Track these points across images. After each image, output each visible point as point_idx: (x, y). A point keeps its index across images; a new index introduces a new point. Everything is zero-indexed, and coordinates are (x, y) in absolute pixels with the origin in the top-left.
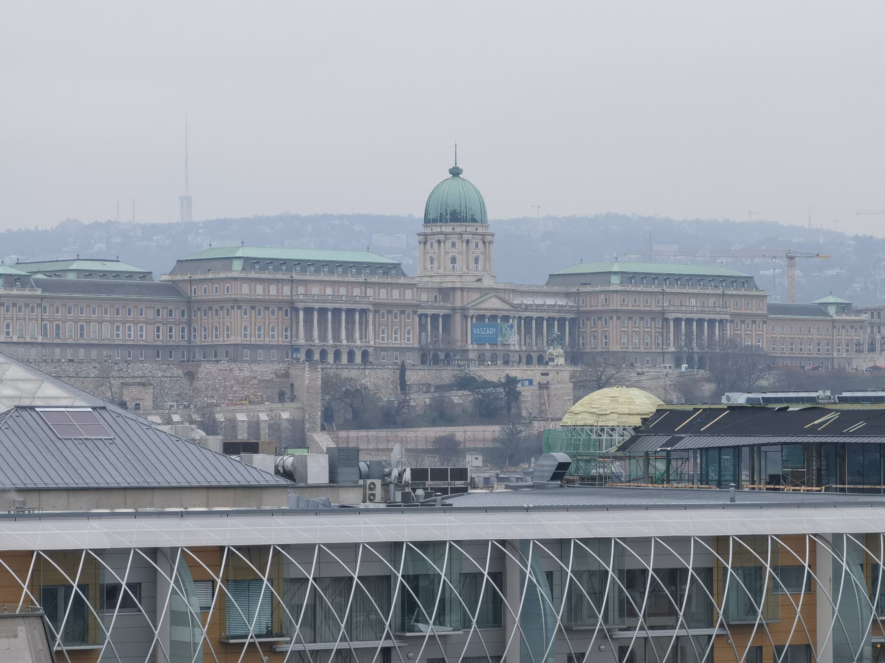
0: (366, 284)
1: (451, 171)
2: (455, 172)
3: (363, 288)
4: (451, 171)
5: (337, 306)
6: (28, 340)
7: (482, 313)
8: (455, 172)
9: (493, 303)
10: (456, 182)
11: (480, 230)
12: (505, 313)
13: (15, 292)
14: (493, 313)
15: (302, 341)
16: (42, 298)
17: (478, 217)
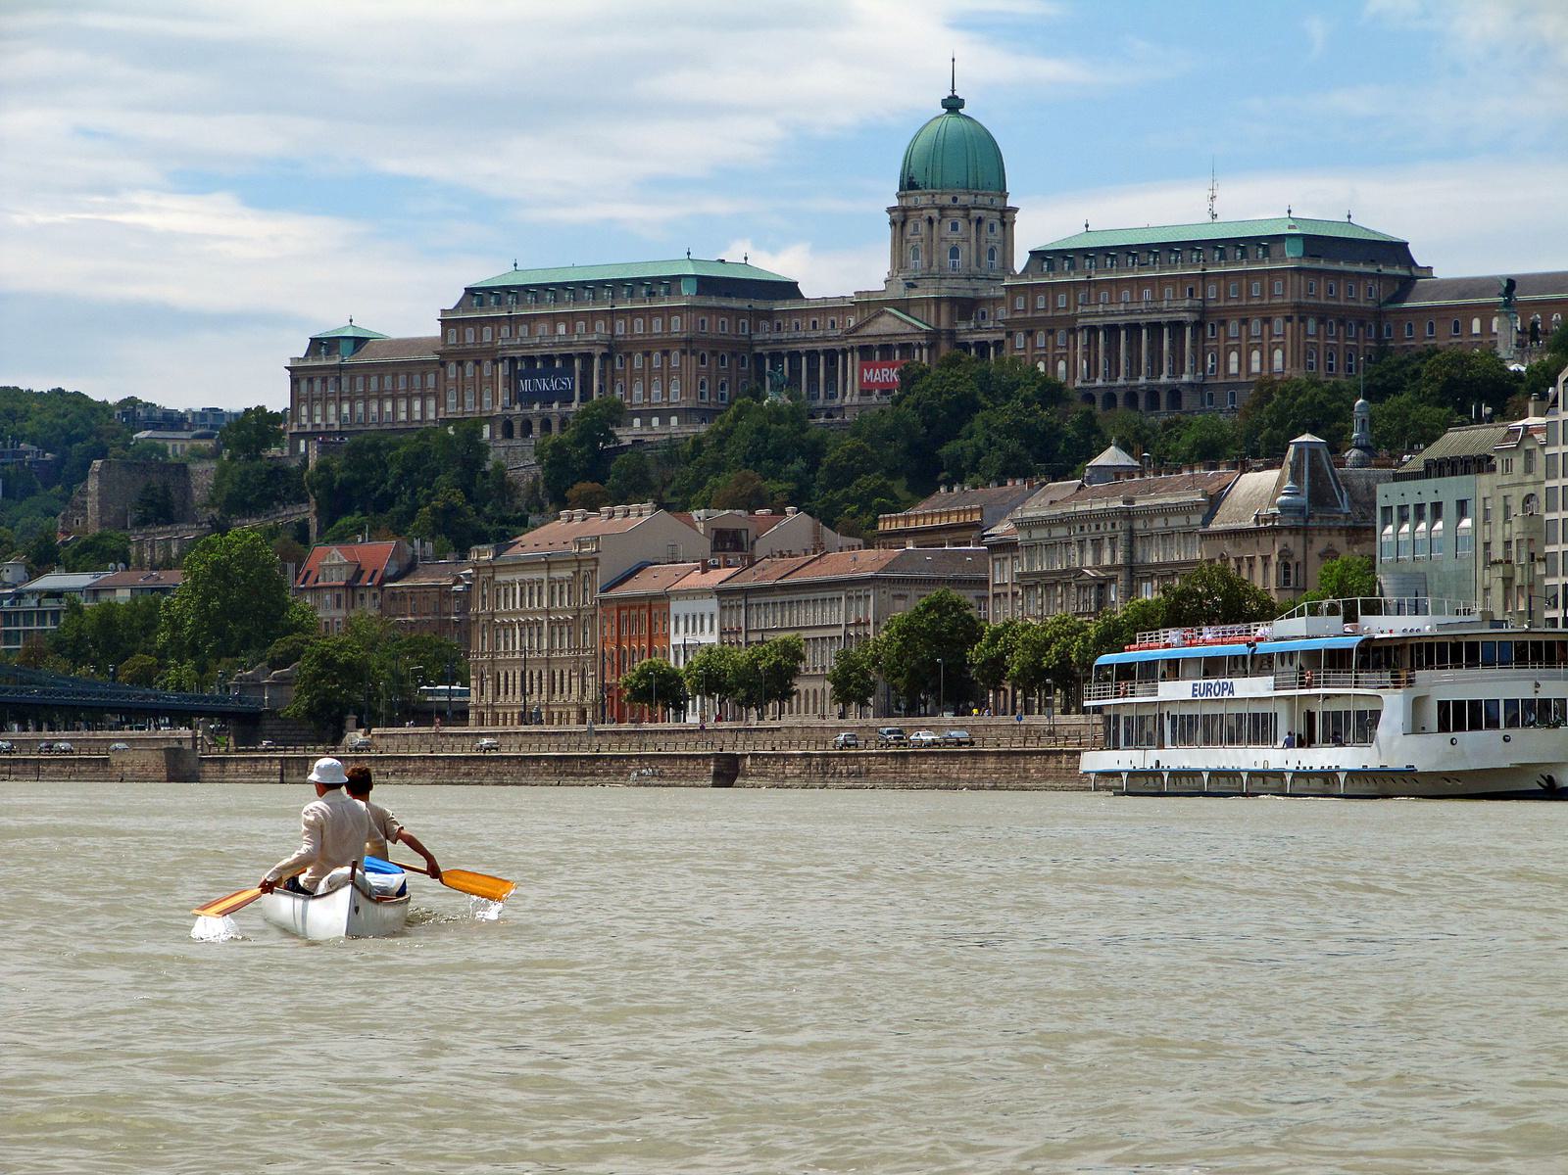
0: (613, 314)
1: (945, 103)
2: (953, 104)
3: (629, 319)
4: (945, 103)
5: (547, 351)
6: (323, 428)
7: (867, 342)
8: (953, 104)
9: (887, 325)
10: (952, 120)
11: (923, 201)
12: (905, 340)
13: (309, 363)
14: (885, 340)
15: (499, 410)
16: (340, 367)
17: (917, 180)
